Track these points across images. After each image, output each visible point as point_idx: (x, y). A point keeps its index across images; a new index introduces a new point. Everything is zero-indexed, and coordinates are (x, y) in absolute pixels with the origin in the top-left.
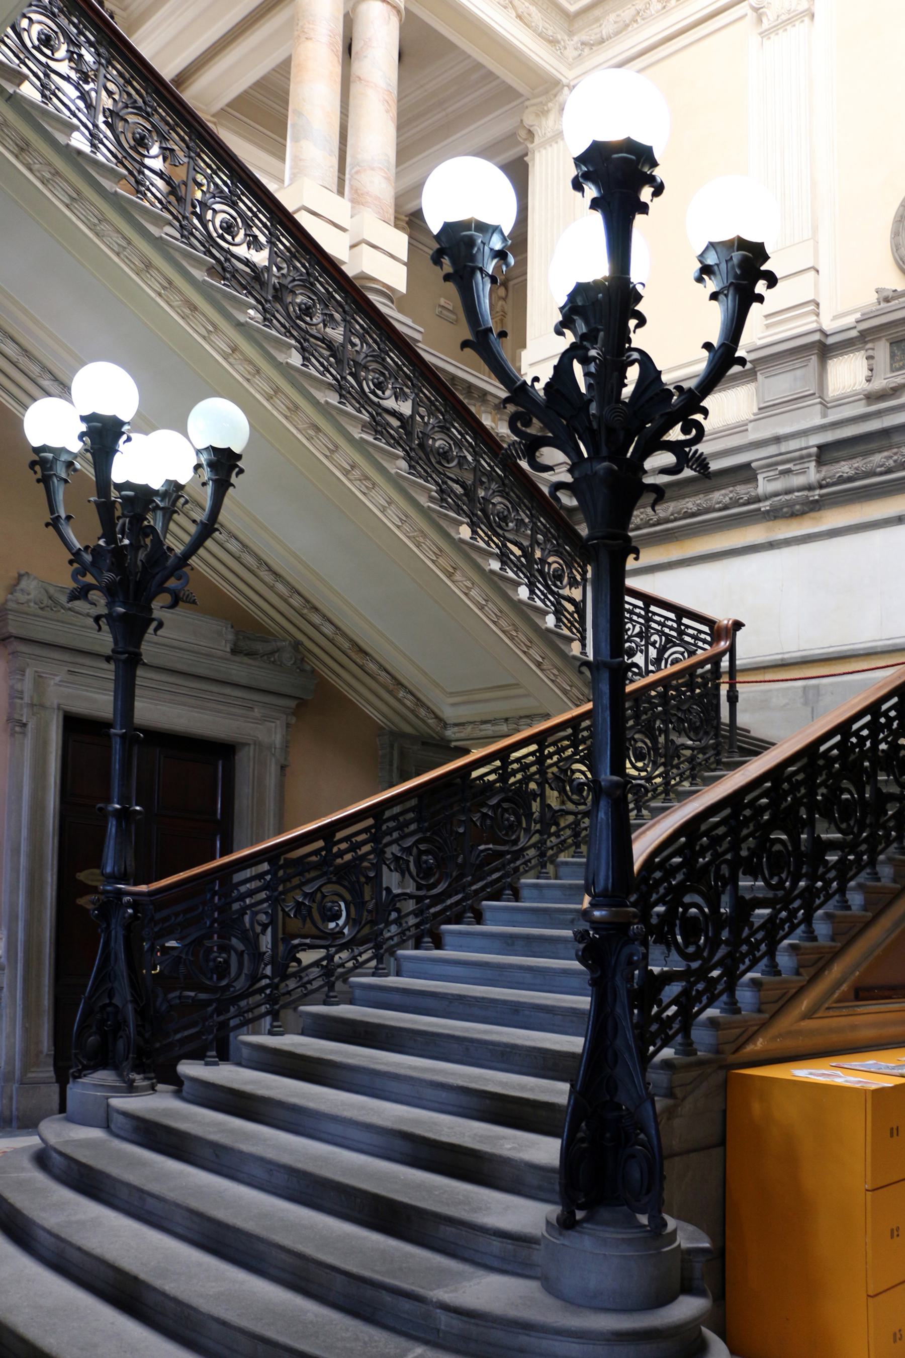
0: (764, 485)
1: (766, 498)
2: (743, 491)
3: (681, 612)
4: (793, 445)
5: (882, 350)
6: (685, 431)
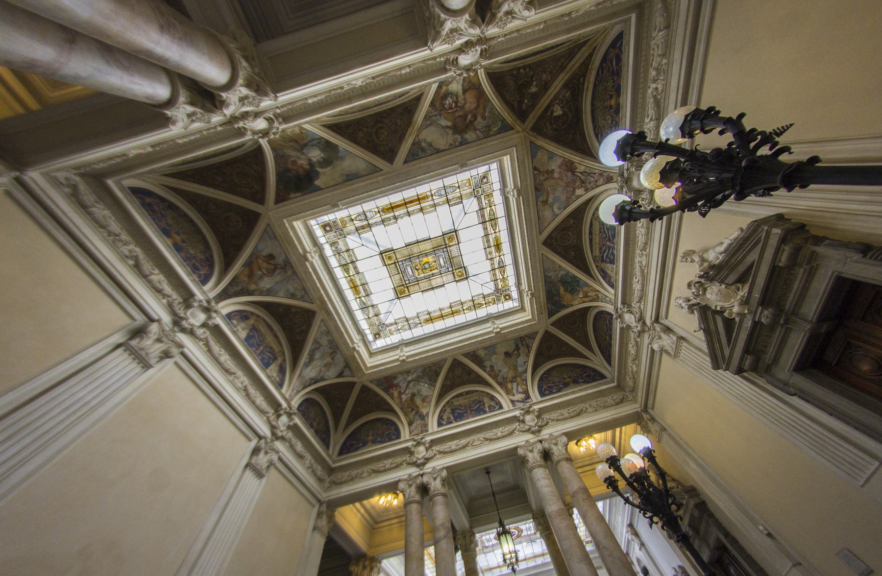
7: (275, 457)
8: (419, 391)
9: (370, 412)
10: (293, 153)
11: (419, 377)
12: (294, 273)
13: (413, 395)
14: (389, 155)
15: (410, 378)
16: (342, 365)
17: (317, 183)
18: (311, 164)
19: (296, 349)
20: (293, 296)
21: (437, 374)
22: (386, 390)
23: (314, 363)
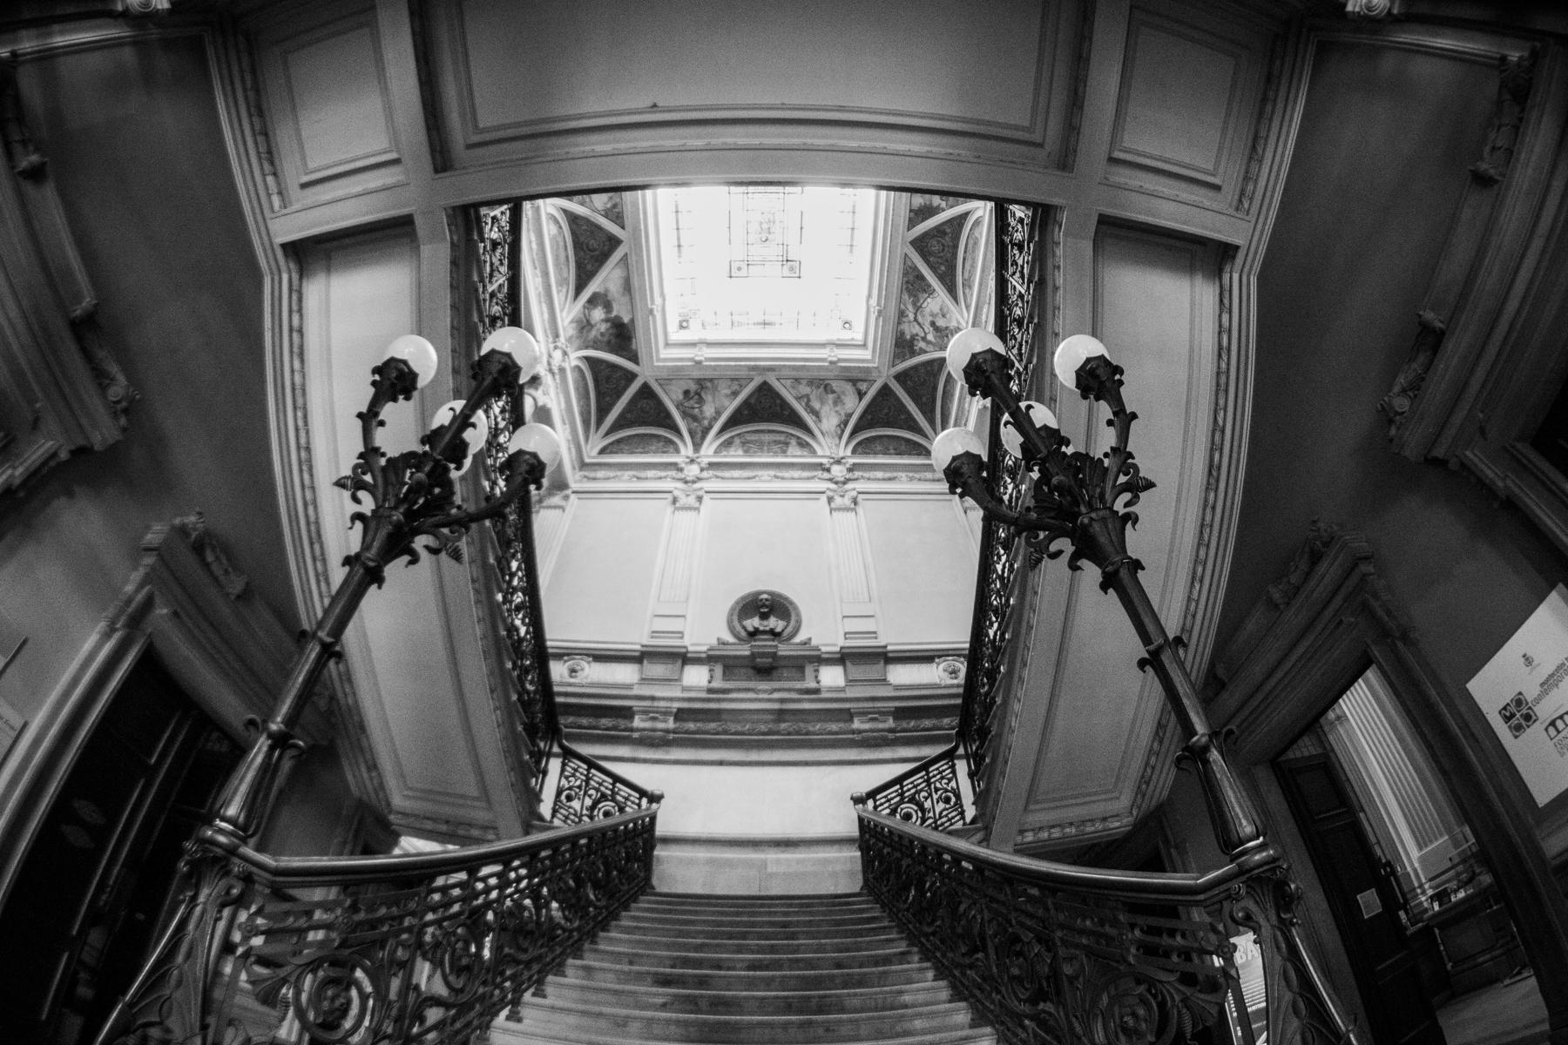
0: (638, 722)
1: (638, 730)
2: (622, 723)
3: (617, 779)
4: (662, 704)
5: (719, 670)
6: (1126, 474)
7: (854, 493)
8: (932, 315)
9: (935, 389)
10: (594, 333)
11: (914, 304)
12: (711, 380)
13: (933, 324)
14: (614, 242)
15: (911, 316)
16: (849, 387)
17: (626, 320)
18: (606, 320)
19: (796, 421)
20: (735, 394)
21: (921, 277)
22: (913, 353)
23: (823, 413)
